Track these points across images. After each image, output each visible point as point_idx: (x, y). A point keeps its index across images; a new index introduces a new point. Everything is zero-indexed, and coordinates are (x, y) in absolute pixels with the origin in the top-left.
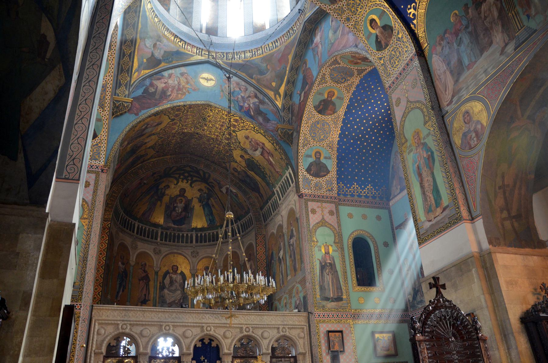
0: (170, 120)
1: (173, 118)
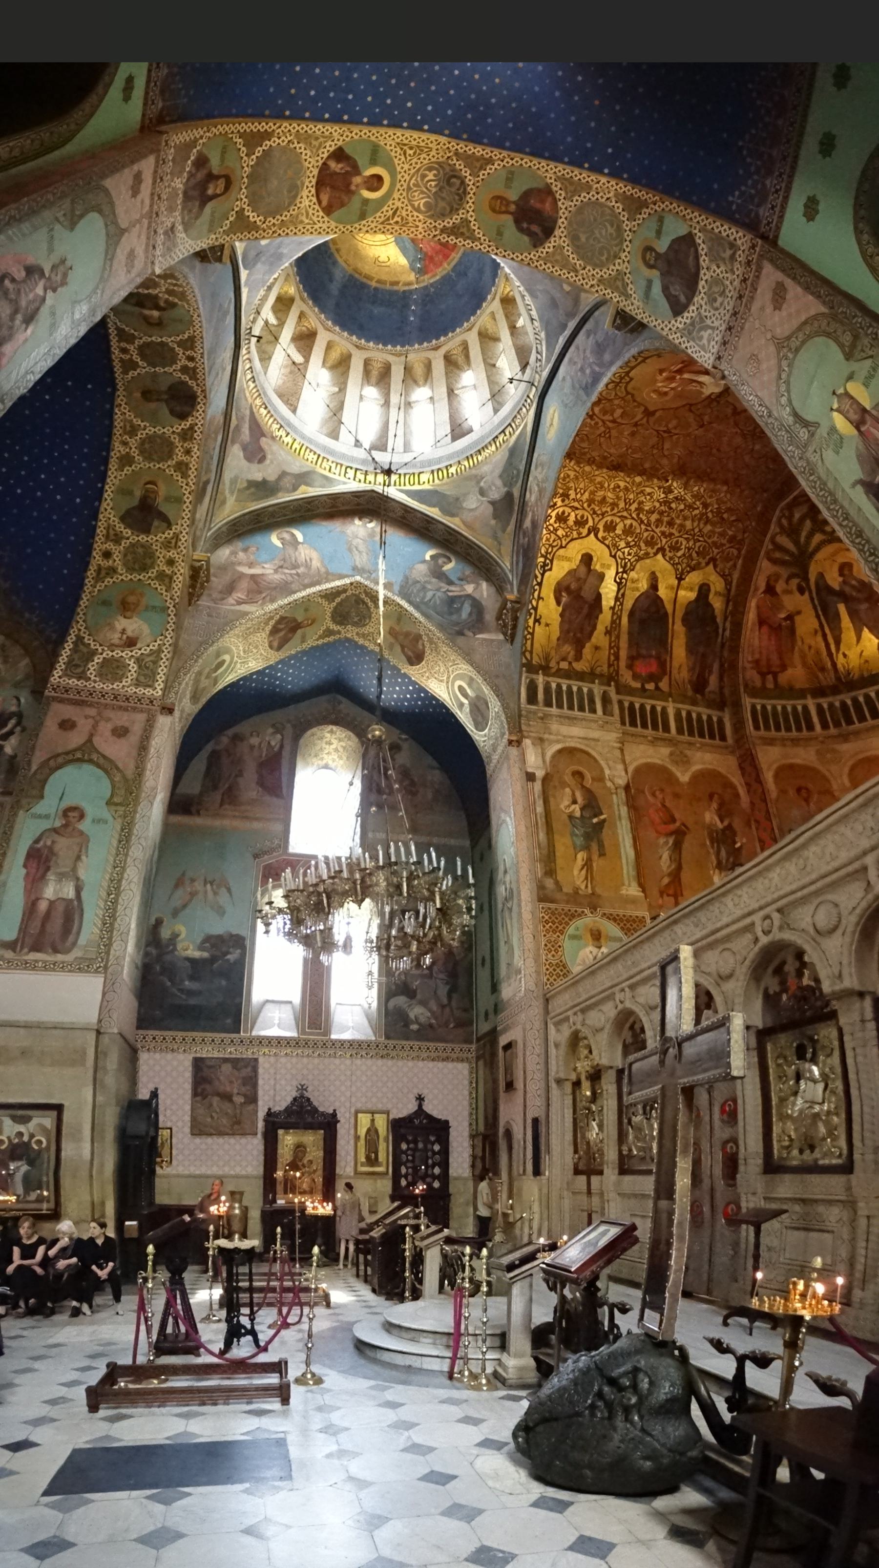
0: (592, 535)
1: (584, 531)
